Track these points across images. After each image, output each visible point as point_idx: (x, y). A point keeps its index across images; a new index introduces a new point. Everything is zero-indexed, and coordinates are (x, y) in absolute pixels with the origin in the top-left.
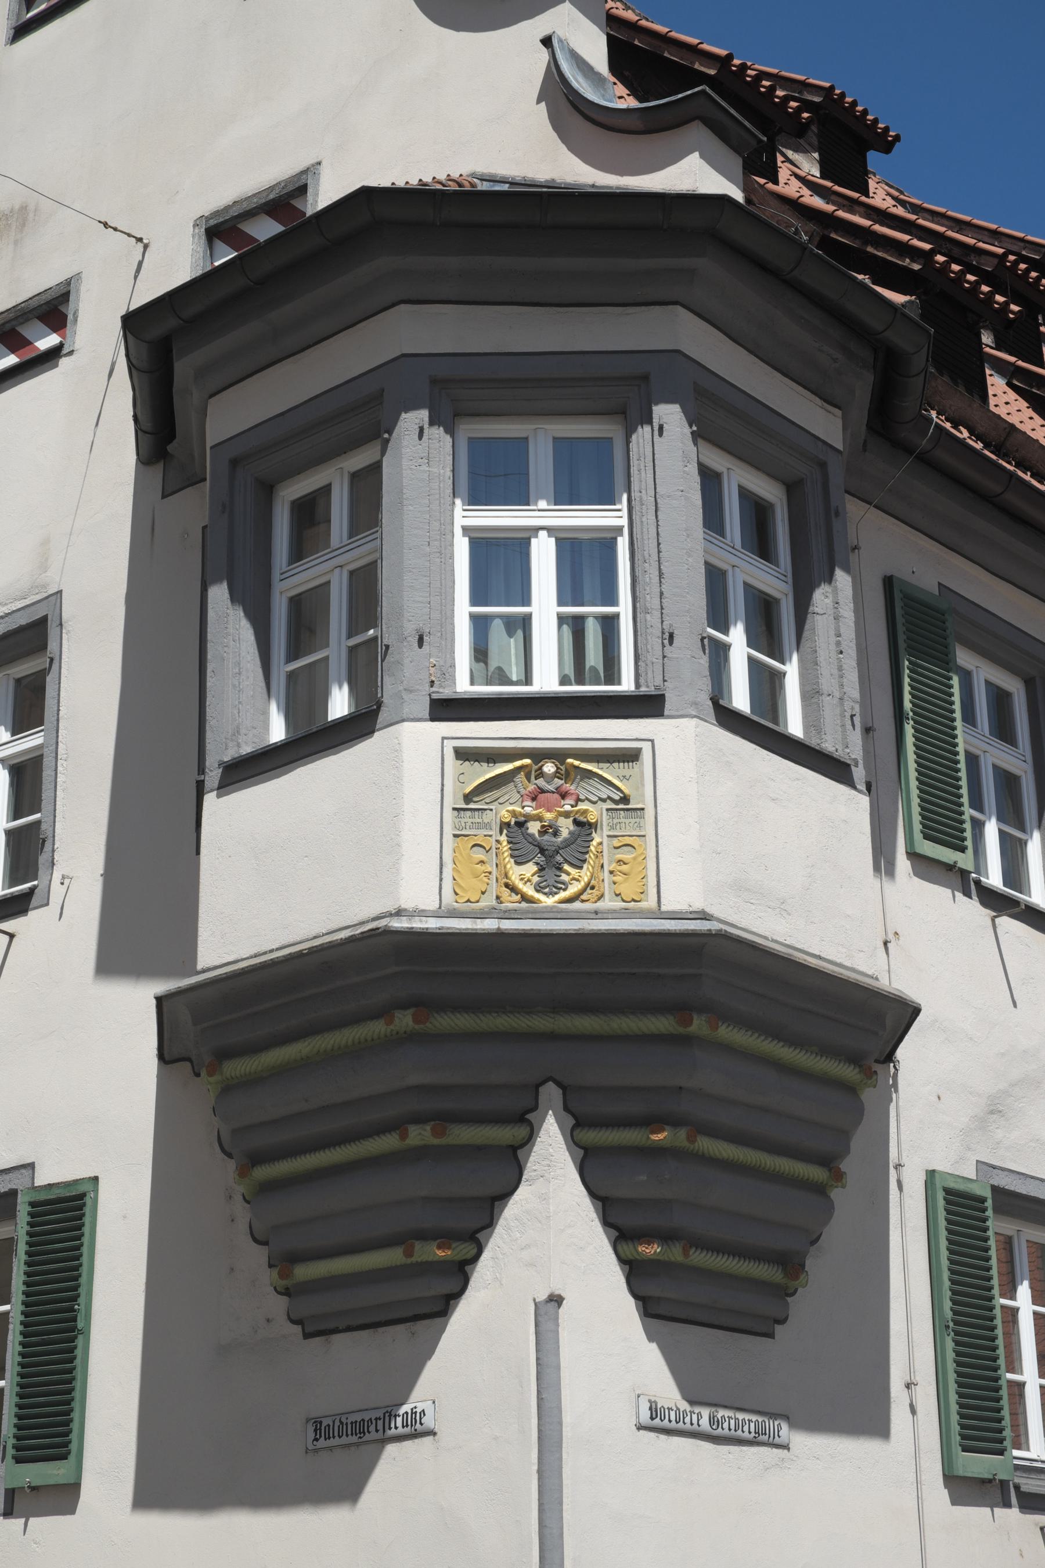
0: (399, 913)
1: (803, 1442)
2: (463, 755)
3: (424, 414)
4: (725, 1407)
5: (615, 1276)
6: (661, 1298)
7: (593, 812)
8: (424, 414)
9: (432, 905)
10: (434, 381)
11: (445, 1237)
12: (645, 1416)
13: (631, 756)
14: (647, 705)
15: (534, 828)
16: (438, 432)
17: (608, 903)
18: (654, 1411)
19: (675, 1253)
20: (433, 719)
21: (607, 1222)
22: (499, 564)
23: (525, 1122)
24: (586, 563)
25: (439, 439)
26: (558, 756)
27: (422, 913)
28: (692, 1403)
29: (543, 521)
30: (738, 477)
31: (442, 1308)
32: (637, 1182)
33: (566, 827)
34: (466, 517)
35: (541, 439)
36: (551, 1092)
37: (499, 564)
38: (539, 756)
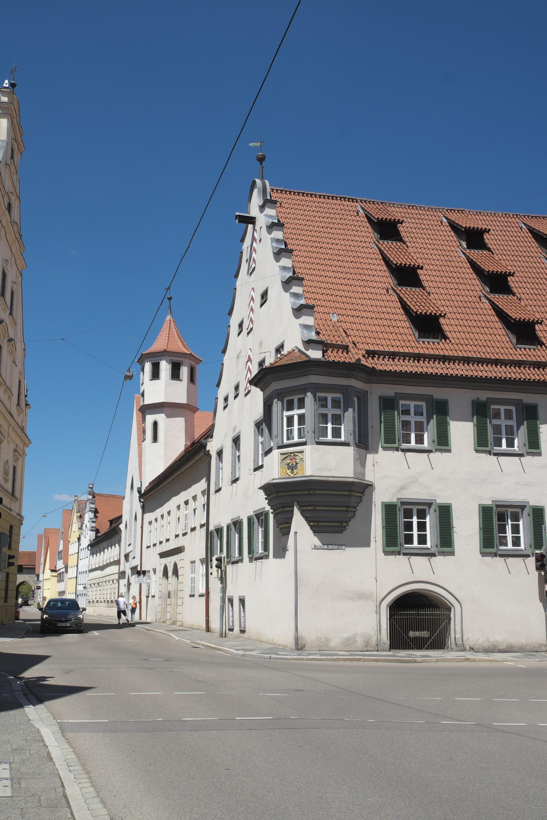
0: (274, 479)
1: (347, 549)
2: (281, 454)
3: (276, 400)
4: (333, 545)
5: (308, 528)
6: (316, 529)
7: (298, 461)
8: (276, 400)
9: (277, 477)
10: (278, 393)
11: (287, 523)
12: (313, 547)
13: (303, 452)
14: (304, 444)
15: (290, 464)
16: (279, 402)
17: (300, 475)
18: (315, 546)
19: (316, 524)
20: (278, 449)
21: (306, 520)
22: (290, 420)
23: (293, 507)
24: (302, 418)
25: (280, 403)
26: (293, 453)
27: (276, 479)
28: (324, 545)
29: (296, 412)
30: (330, 396)
31: (289, 533)
32: (308, 515)
33: (294, 464)
34: (286, 413)
35: (296, 398)
36: (296, 503)
37: (290, 420)
38: (291, 453)
